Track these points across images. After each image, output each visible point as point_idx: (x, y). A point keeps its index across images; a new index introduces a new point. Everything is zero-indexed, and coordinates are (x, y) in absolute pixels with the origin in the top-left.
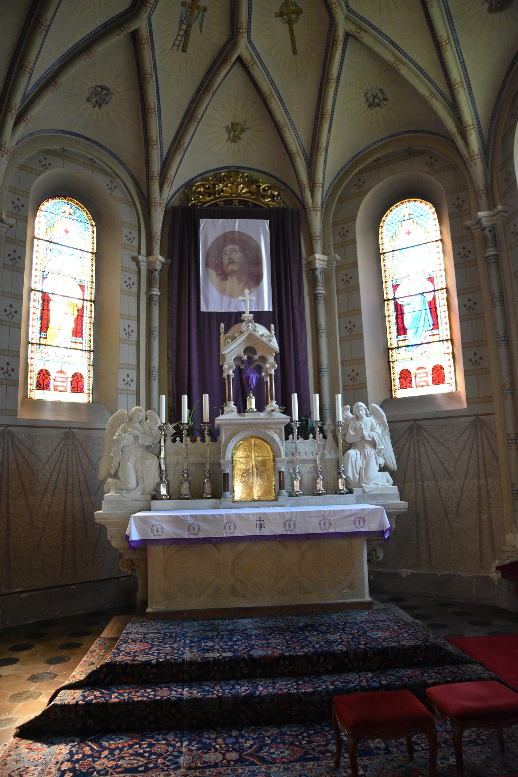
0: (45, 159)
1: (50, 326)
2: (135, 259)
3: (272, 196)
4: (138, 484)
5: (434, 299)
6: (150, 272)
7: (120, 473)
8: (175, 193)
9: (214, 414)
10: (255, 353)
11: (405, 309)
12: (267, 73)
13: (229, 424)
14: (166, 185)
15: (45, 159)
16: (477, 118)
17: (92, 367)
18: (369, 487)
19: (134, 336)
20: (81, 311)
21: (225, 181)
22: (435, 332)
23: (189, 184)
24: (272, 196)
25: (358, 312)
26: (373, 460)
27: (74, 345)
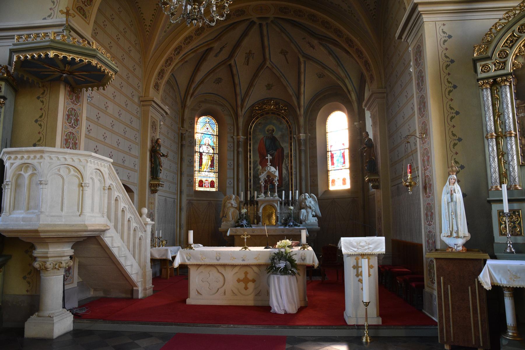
0: (200, 104)
1: (203, 164)
2: (232, 137)
3: (285, 110)
4: (232, 219)
5: (344, 152)
6: (238, 142)
7: (227, 216)
8: (247, 110)
9: (258, 197)
10: (270, 177)
11: (334, 156)
12: (279, 70)
13: (261, 201)
14: (243, 109)
15: (200, 104)
16: (355, 88)
17: (217, 179)
18: (308, 222)
19: (232, 167)
20: (213, 158)
21: (266, 104)
22: (344, 165)
23: (253, 106)
24: (285, 110)
25: (316, 157)
26: (310, 213)
27: (211, 171)
